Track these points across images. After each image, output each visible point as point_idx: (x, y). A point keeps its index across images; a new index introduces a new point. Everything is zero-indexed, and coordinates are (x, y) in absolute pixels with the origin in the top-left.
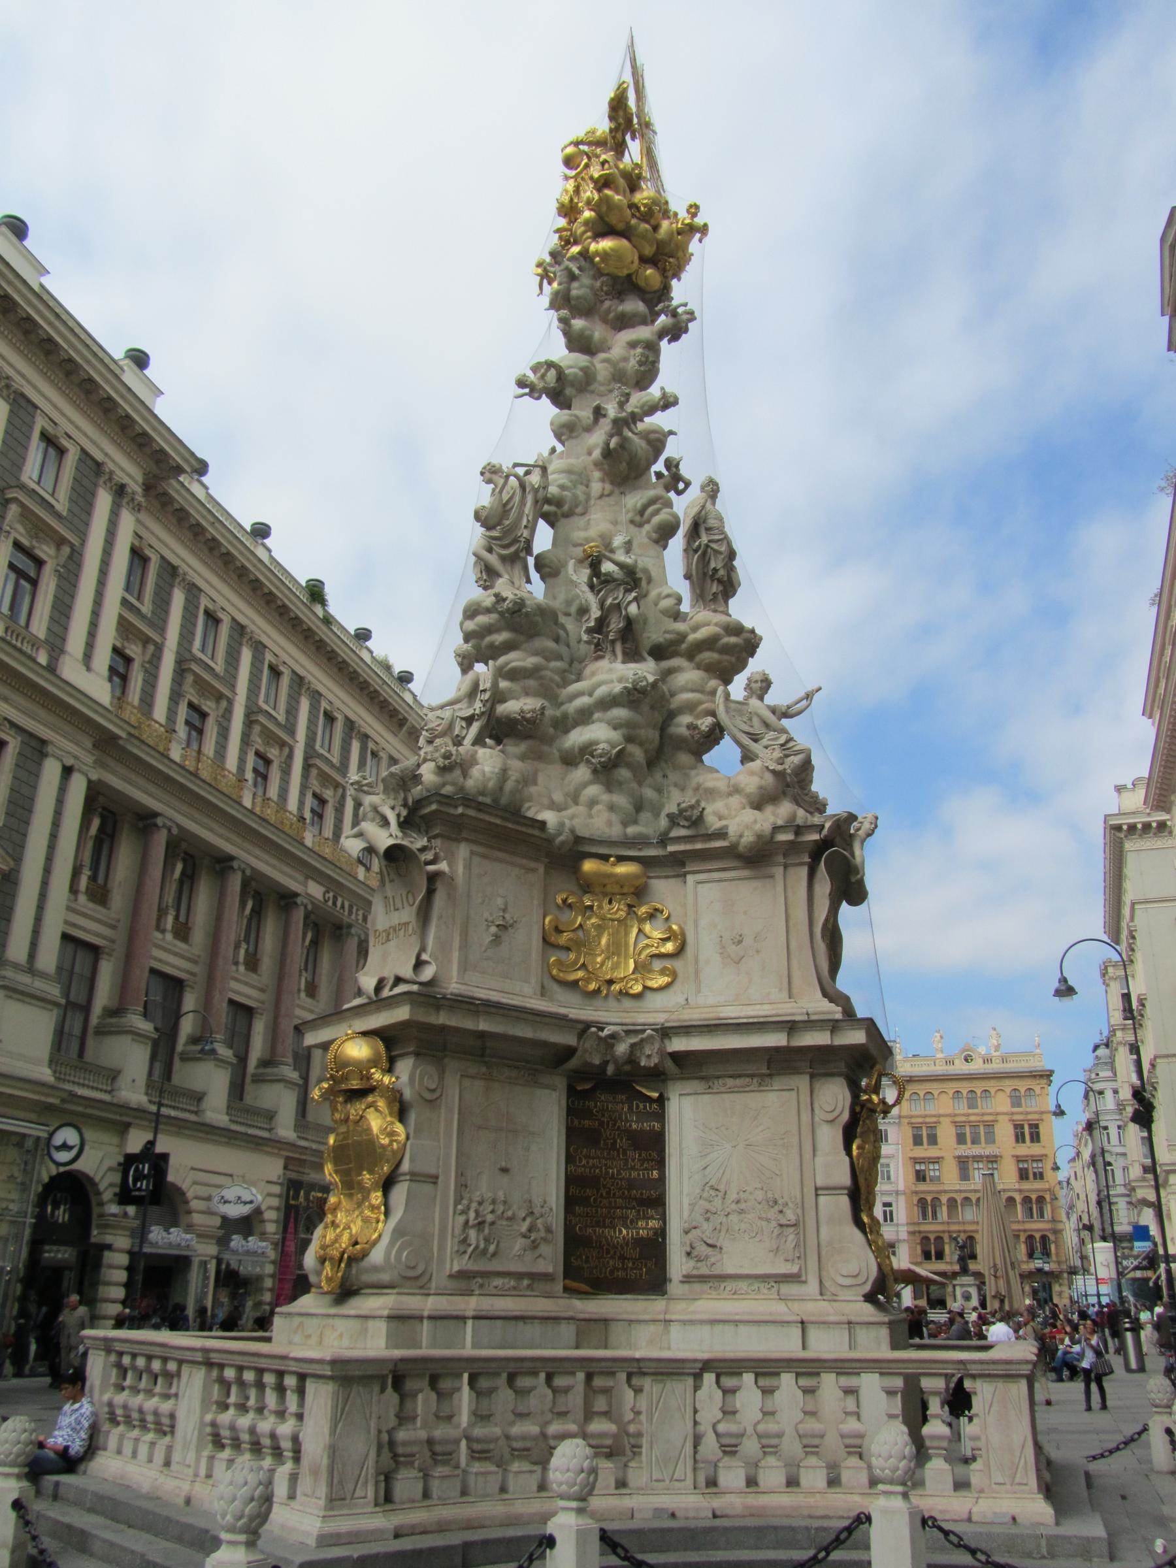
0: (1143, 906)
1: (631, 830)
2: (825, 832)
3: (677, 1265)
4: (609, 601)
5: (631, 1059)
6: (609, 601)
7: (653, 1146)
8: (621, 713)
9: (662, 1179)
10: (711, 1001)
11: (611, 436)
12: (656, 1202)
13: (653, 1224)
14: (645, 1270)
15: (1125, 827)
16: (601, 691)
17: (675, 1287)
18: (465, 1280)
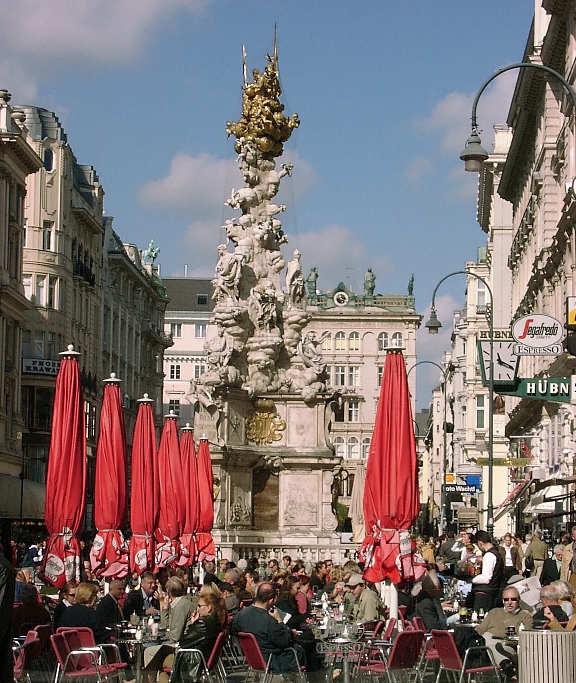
0: (500, 232)
1: (270, 388)
2: (331, 396)
3: (281, 521)
4: (266, 310)
5: (272, 464)
6: (266, 310)
7: (275, 489)
8: (270, 350)
9: (277, 498)
10: (293, 445)
11: (265, 234)
12: (276, 504)
13: (275, 511)
14: (272, 522)
15: (495, 165)
16: (263, 343)
17: (281, 528)
18: (232, 526)
